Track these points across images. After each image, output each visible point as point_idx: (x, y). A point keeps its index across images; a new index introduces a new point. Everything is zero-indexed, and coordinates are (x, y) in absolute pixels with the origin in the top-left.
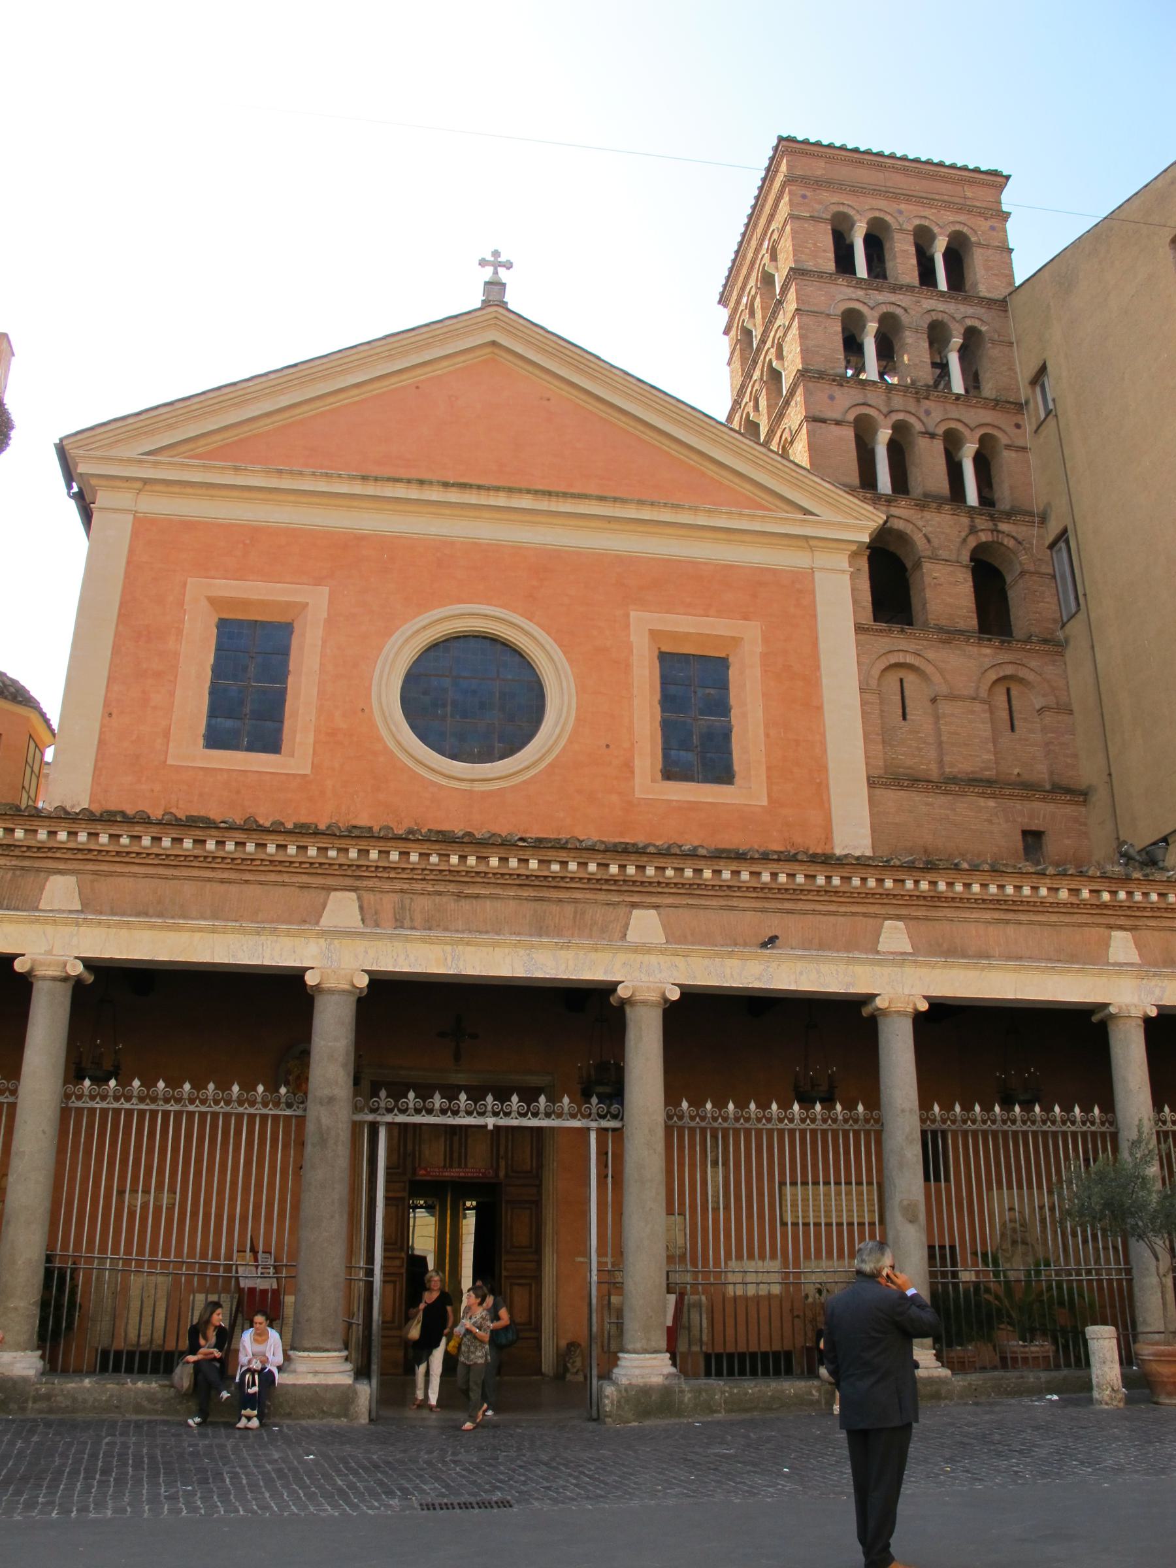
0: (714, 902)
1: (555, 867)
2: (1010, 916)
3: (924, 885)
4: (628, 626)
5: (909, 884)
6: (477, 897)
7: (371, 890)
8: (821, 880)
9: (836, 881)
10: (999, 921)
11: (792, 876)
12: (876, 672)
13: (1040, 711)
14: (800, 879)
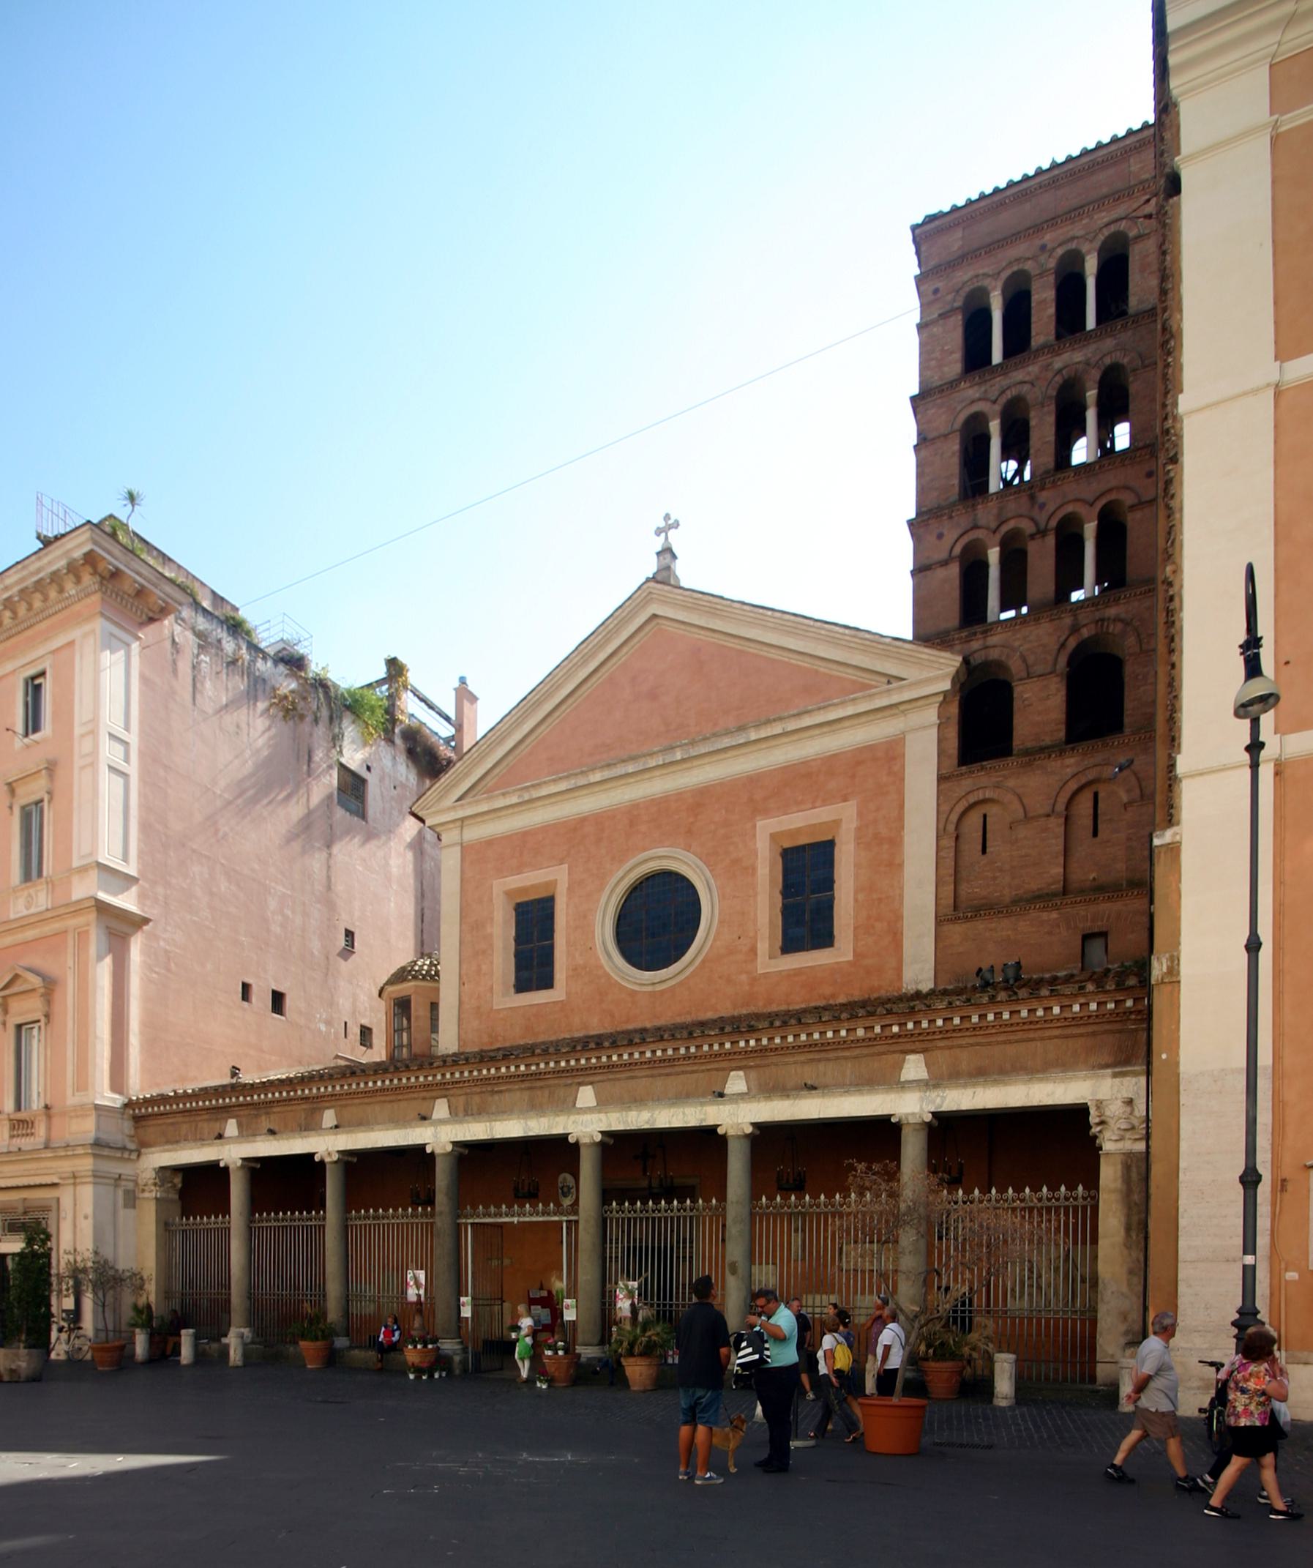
0: (623, 1075)
1: (533, 1068)
2: (823, 1055)
3: (752, 1043)
4: (754, 836)
5: (742, 1044)
6: (501, 1092)
7: (452, 1095)
8: (682, 1051)
9: (693, 1050)
10: (812, 1060)
11: (664, 1050)
12: (954, 817)
13: (1125, 806)
14: (670, 1052)
